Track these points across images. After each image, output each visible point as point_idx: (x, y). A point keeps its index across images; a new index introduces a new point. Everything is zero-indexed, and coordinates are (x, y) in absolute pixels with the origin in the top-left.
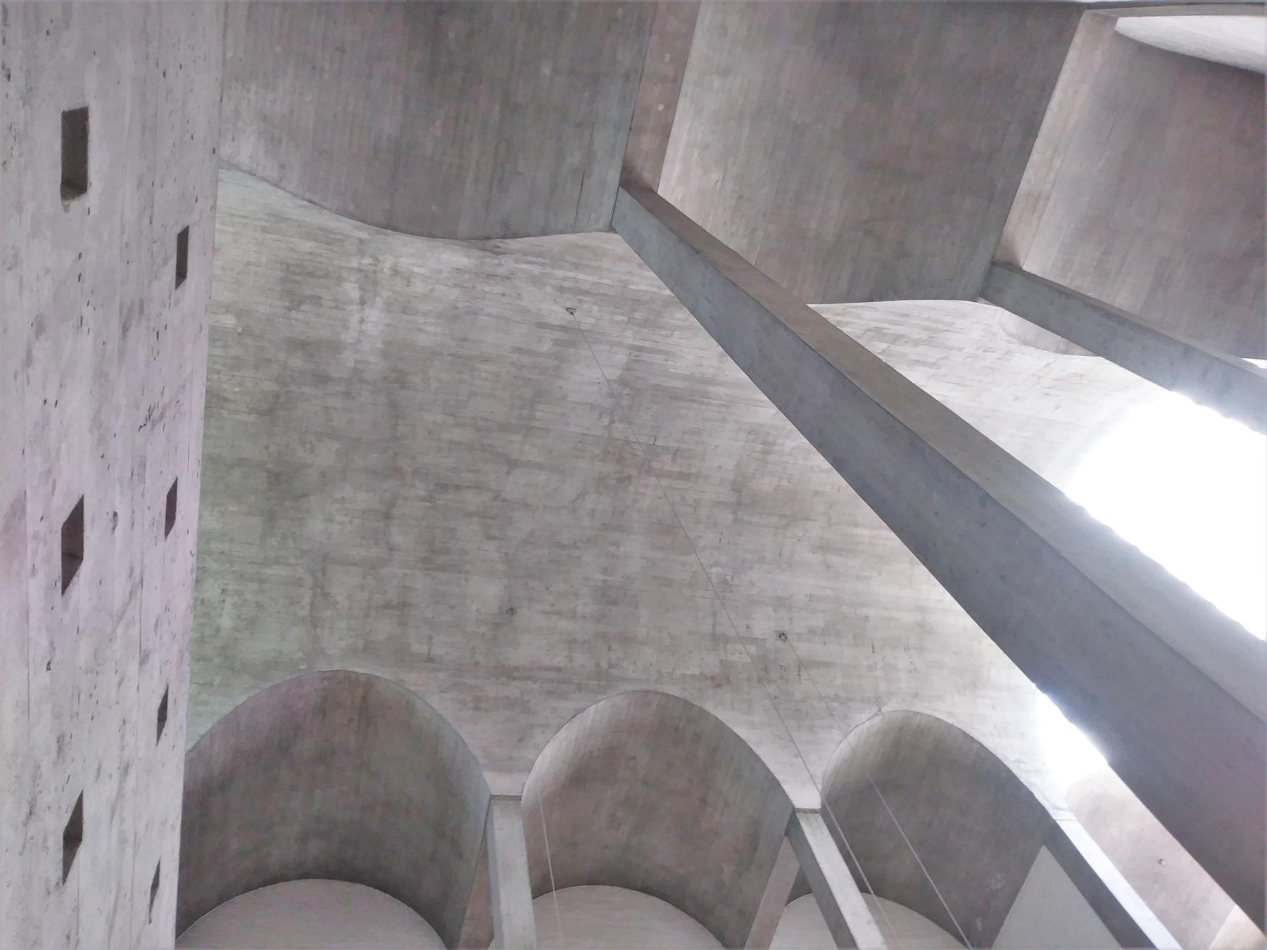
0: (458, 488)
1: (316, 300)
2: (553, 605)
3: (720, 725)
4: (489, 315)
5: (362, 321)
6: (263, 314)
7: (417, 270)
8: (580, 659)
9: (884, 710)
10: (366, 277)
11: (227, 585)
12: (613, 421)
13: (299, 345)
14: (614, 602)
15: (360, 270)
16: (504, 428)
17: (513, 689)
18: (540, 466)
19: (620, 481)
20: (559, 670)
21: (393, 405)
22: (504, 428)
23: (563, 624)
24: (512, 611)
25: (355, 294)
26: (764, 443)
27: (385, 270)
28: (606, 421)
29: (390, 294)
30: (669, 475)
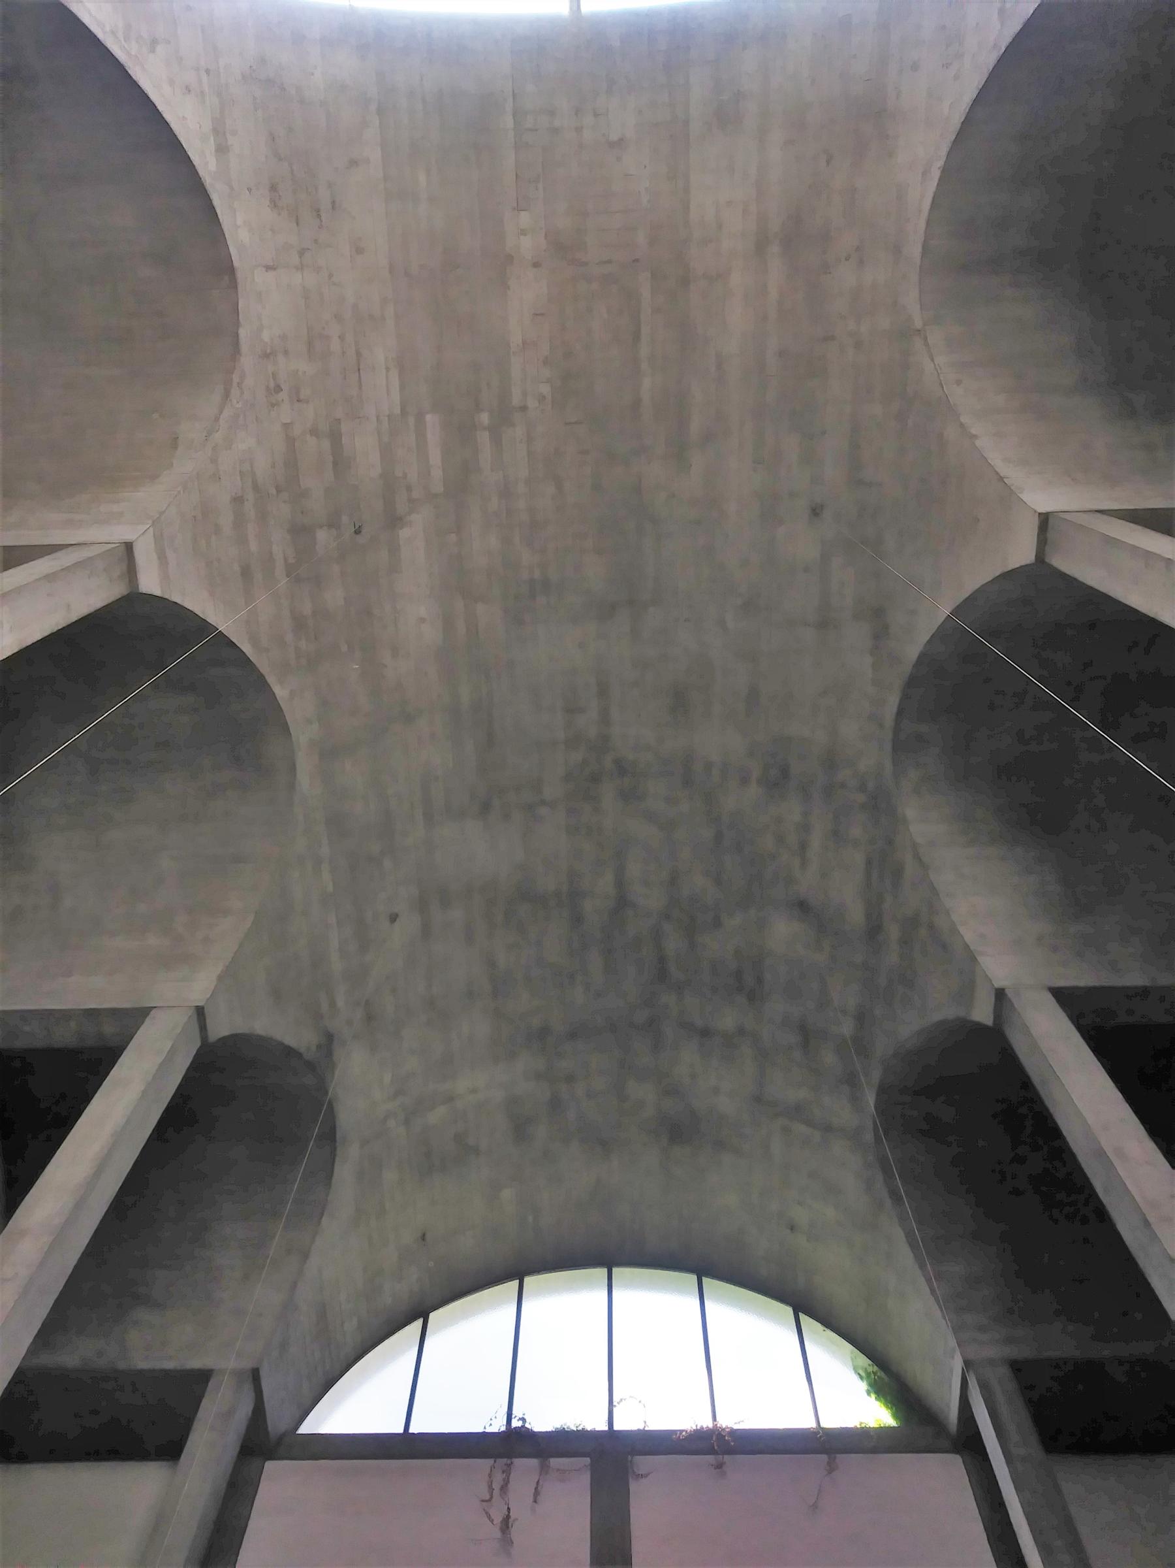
0: (662, 960)
3: (942, 634)
7: (387, 1078)
8: (856, 832)
9: (918, 324)
12: (543, 803)
14: (785, 772)
15: (407, 1122)
16: (577, 919)
17: (893, 932)
20: (869, 862)
21: (573, 1035)
22: (577, 919)
23: (816, 842)
24: (802, 907)
28: (543, 811)
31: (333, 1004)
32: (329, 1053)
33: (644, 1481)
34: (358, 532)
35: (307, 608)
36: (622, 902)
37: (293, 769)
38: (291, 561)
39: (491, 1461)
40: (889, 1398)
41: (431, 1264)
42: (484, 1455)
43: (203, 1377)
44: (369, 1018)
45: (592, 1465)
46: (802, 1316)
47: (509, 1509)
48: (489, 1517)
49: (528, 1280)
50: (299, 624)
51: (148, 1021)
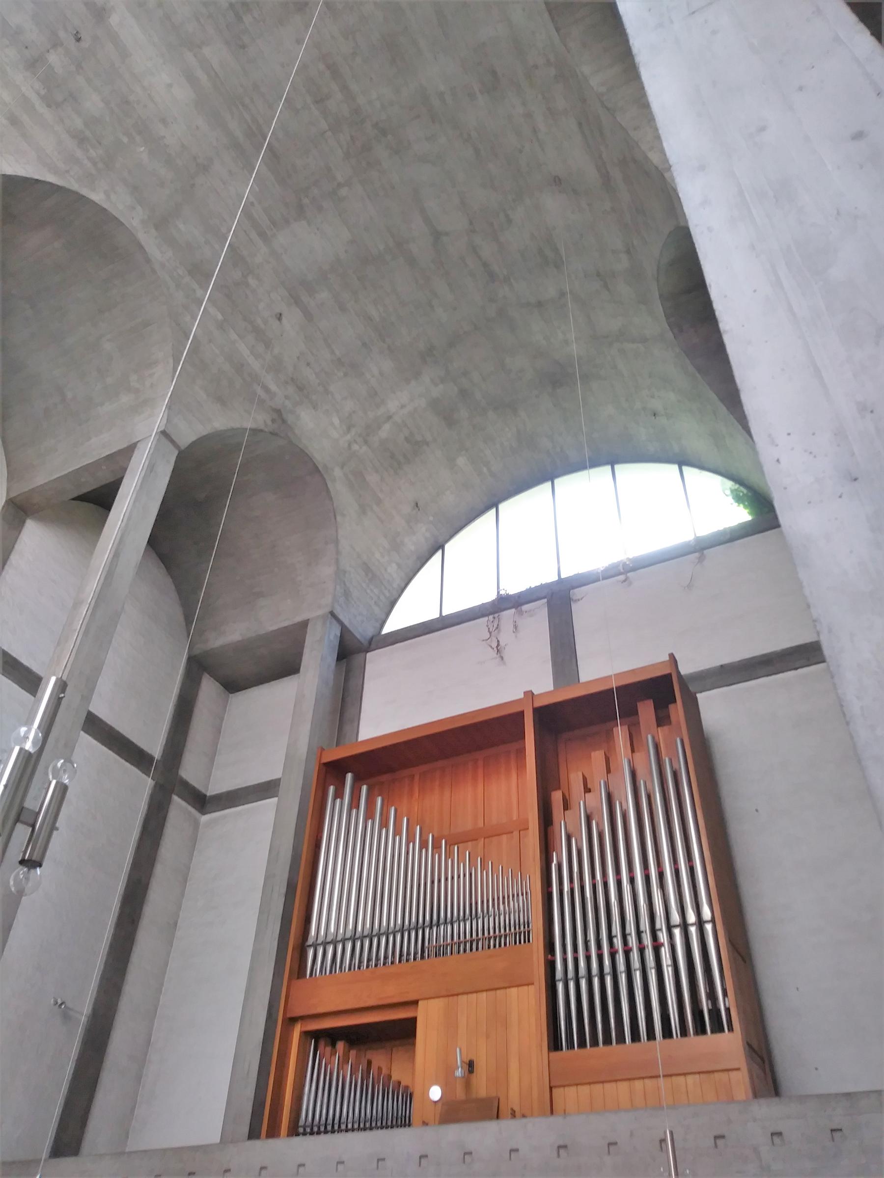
0: (485, 265)
1: (407, 439)
4: (333, 352)
7: (336, 421)
12: (340, 185)
13: (449, 419)
14: (494, 73)
15: (366, 442)
19: (384, 133)
20: (580, 124)
24: (557, 181)
25: (387, 427)
26: (239, 19)
28: (344, 192)
30: (344, 88)
31: (266, 389)
32: (284, 421)
33: (581, 601)
34: (78, 40)
35: (79, 123)
36: (437, 235)
37: (141, 247)
38: (43, 92)
39: (486, 619)
40: (746, 503)
41: (431, 518)
42: (483, 616)
43: (304, 625)
44: (300, 388)
45: (548, 602)
46: (685, 468)
47: (498, 641)
48: (491, 647)
49: (502, 506)
50: (81, 140)
51: (136, 452)
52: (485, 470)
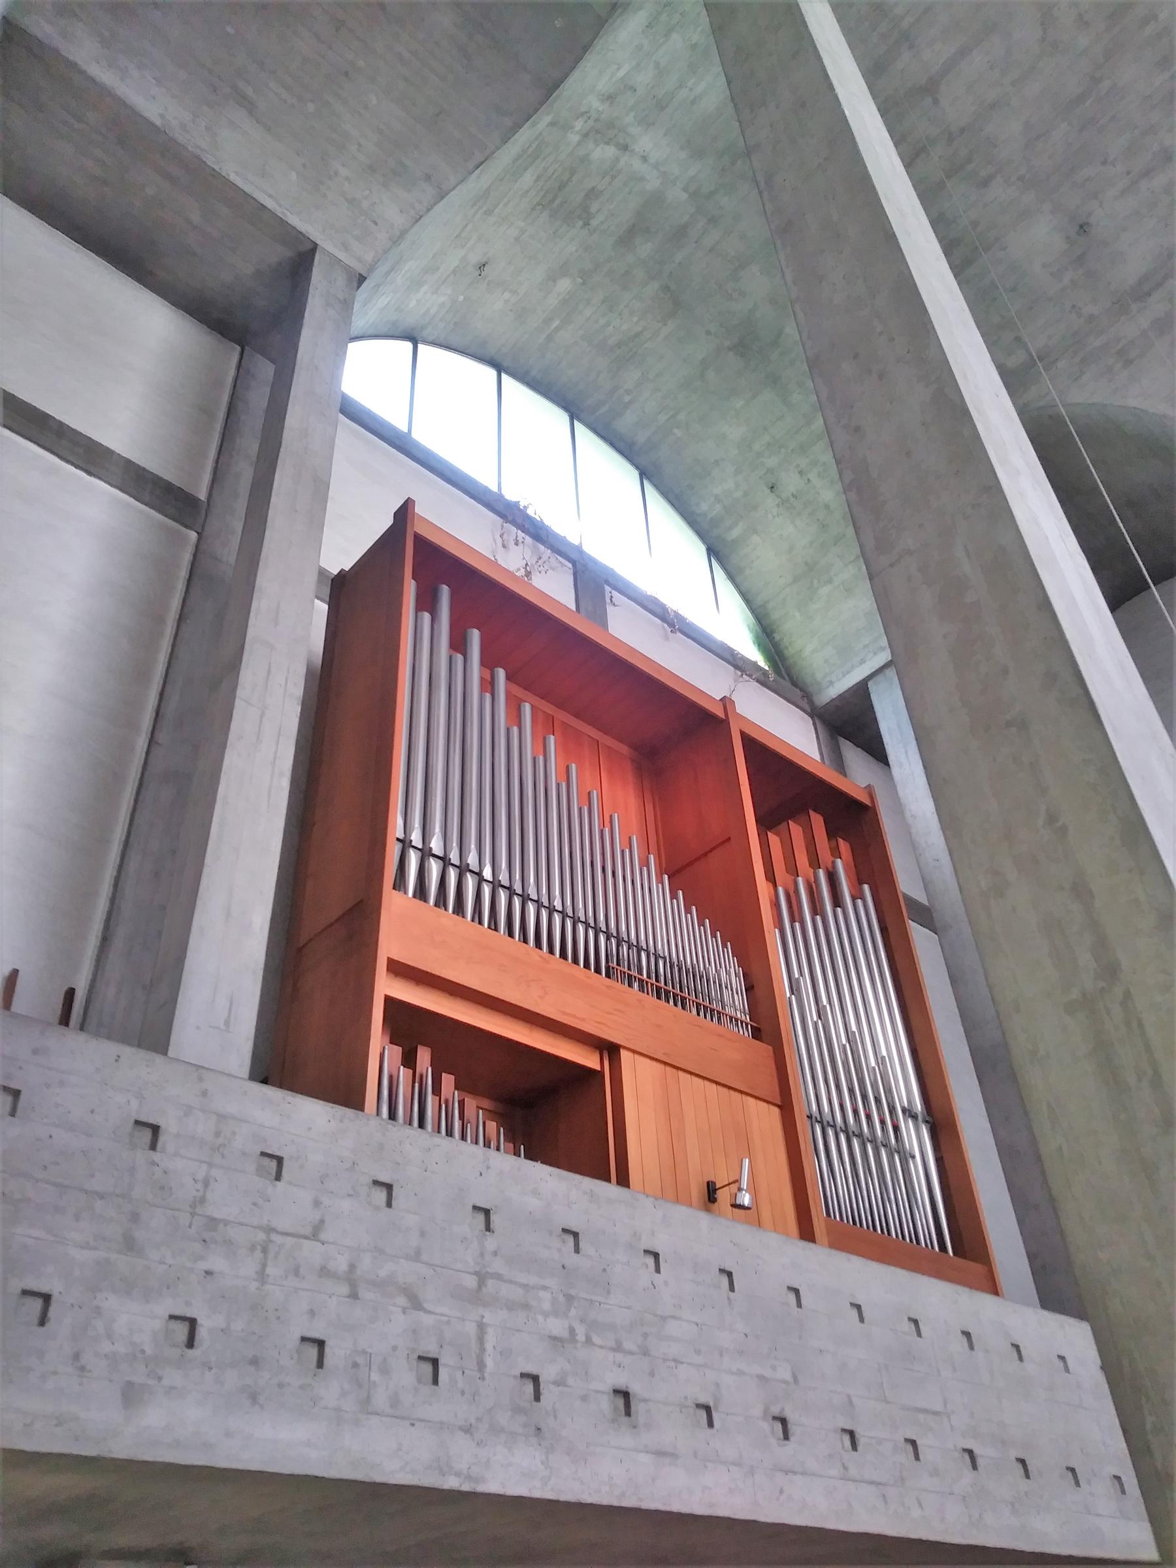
1: (592, 194)
2: (1128, 173)
5: (644, 159)
6: (577, 251)
7: (621, 74)
10: (598, 132)
11: (798, 466)
18: (963, 52)
24: (1083, 228)
25: (610, 151)
27: (600, 109)
29: (632, 114)
36: (930, 88)
52: (556, 323)
